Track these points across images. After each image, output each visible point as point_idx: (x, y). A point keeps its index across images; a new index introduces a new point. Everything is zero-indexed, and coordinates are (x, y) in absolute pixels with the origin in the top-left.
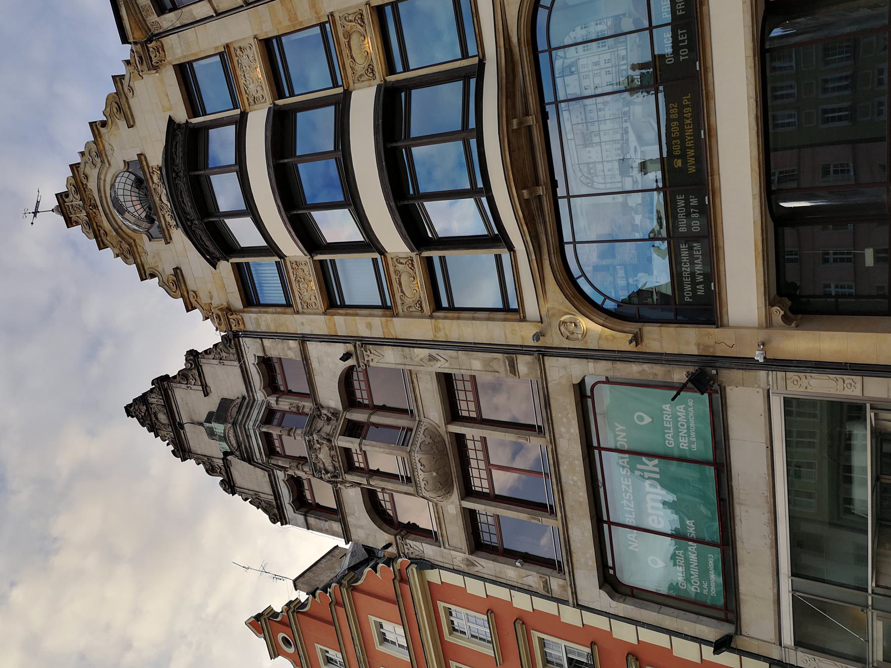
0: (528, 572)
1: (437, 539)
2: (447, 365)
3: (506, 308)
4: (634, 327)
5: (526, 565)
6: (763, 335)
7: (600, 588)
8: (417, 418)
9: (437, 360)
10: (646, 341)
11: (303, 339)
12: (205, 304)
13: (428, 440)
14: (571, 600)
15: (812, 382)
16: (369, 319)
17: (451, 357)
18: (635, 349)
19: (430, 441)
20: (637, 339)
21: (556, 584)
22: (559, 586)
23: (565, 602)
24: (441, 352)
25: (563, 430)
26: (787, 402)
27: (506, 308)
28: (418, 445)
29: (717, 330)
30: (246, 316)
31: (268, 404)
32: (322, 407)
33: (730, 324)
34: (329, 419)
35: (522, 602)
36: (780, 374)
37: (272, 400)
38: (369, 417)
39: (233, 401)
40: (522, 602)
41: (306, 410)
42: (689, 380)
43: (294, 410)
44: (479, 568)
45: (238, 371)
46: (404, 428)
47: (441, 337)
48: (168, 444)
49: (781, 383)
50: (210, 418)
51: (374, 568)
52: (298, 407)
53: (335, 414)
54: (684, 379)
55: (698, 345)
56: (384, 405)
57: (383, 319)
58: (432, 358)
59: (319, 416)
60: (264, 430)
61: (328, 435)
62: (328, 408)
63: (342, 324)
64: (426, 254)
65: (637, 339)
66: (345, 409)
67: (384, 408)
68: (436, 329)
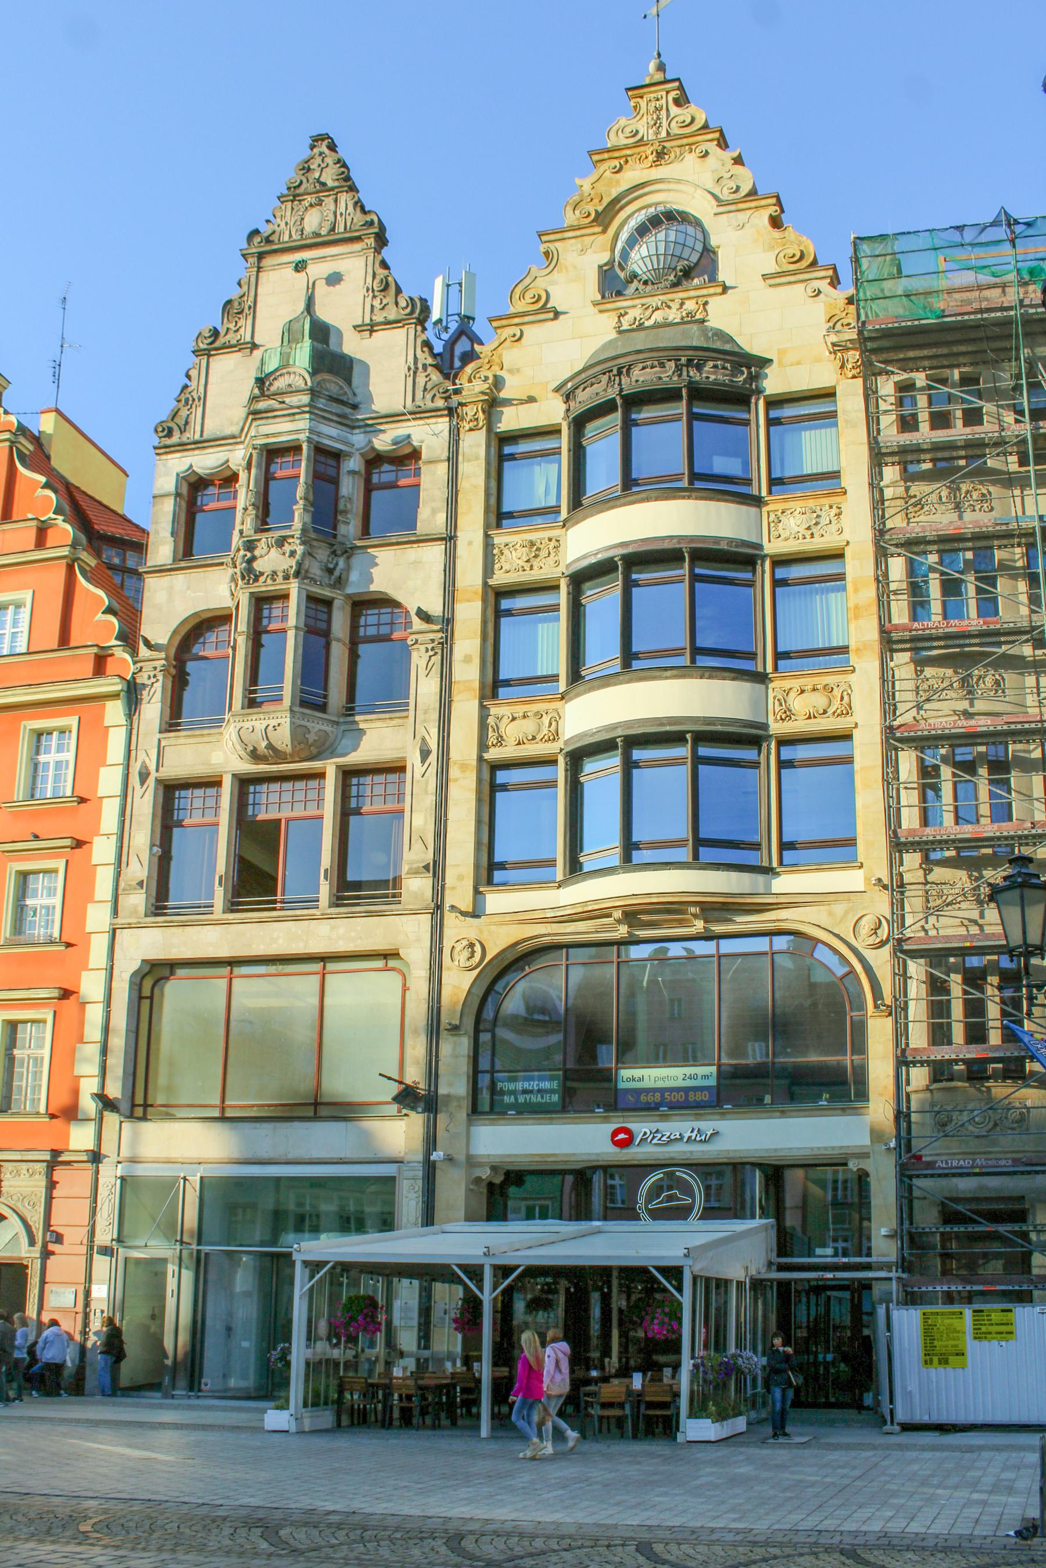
0: (146, 863)
1: (171, 725)
2: (418, 775)
3: (493, 866)
4: (469, 1024)
5: (156, 860)
6: (461, 1158)
7: (143, 961)
8: (342, 720)
9: (423, 761)
10: (452, 1039)
11: (450, 539)
12: (500, 356)
13: (312, 737)
14: (119, 921)
15: (413, 1203)
16: (477, 661)
17: (427, 783)
18: (442, 1027)
19: (311, 741)
20: (455, 1029)
21: (137, 901)
22: (136, 907)
23: (115, 912)
24: (433, 770)
25: (341, 931)
26: (392, 1180)
27: (493, 866)
28: (303, 723)
29: (465, 1115)
30: (481, 436)
31: (349, 455)
32: (348, 558)
33: (473, 1128)
34: (330, 571)
35: (103, 850)
36: (420, 1174)
37: (354, 463)
38: (339, 640)
39: (349, 381)
40: (103, 850)
41: (342, 529)
42: (408, 1086)
43: (341, 506)
44: (139, 791)
45: (399, 408)
46: (325, 697)
47: (454, 772)
48: (268, 221)
49: (411, 1174)
50: (321, 332)
51: (109, 611)
52: (345, 512)
53: (339, 583)
54: (409, 1080)
55: (448, 1096)
56: (358, 656)
57: (477, 685)
58: (425, 754)
59: (334, 553)
60: (305, 447)
61: (307, 571)
62: (348, 568)
63: (470, 614)
64: (561, 760)
65: (455, 1029)
66: (349, 596)
67: (354, 657)
68: (463, 767)
